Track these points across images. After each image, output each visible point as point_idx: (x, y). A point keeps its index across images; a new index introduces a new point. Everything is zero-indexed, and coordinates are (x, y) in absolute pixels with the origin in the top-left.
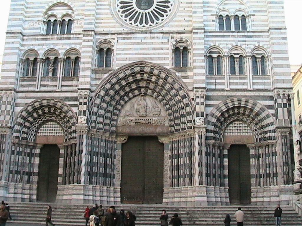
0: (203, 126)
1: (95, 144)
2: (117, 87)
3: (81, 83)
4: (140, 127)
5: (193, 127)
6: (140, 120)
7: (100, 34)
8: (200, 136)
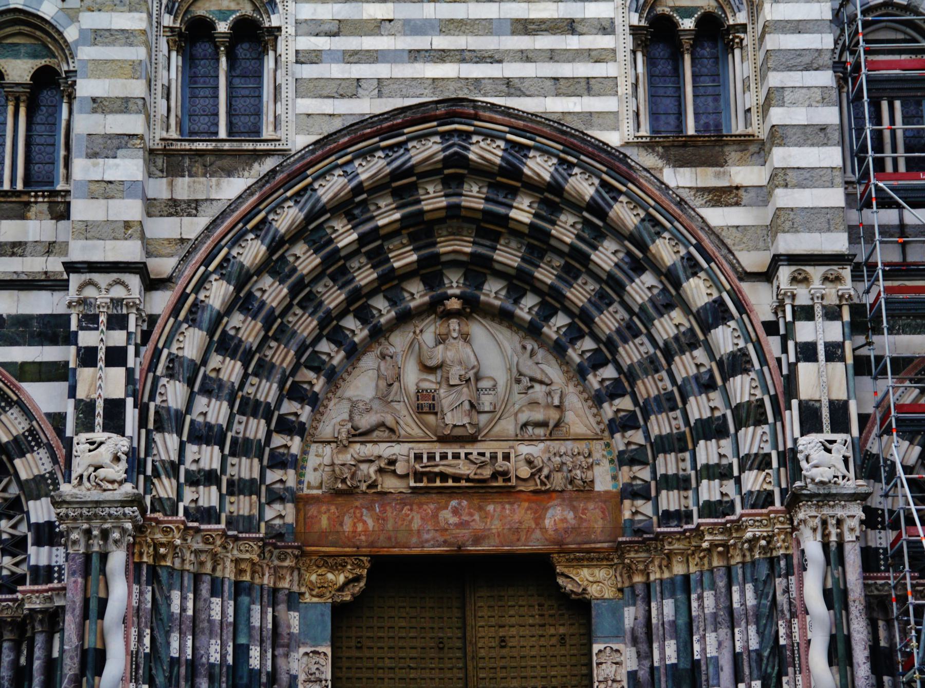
0: (852, 485)
1: (175, 608)
2: (305, 260)
3: (88, 230)
4: (443, 500)
5: (783, 492)
6: (444, 457)
8: (833, 546)
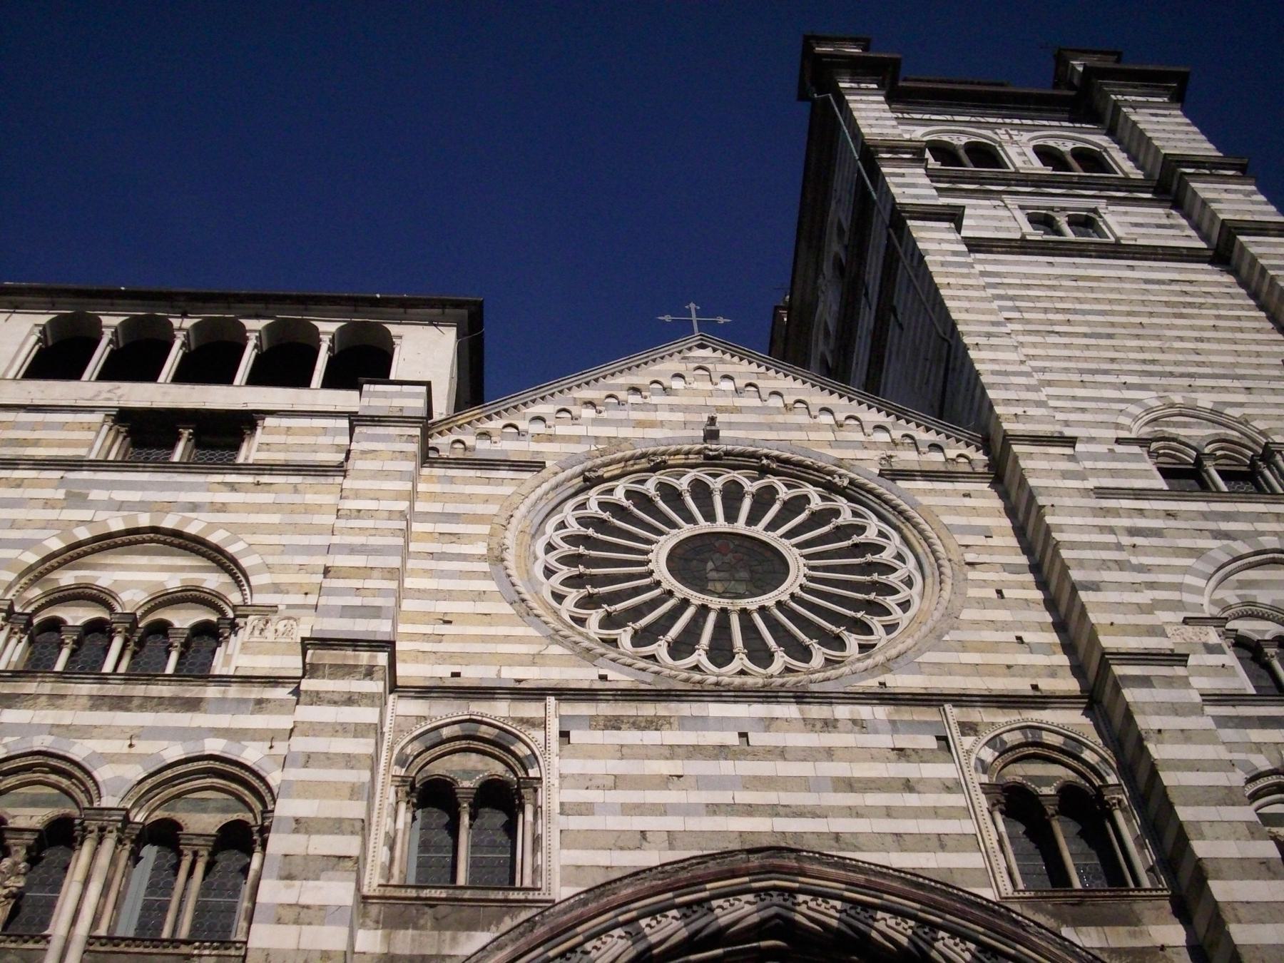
7: (426, 692)
